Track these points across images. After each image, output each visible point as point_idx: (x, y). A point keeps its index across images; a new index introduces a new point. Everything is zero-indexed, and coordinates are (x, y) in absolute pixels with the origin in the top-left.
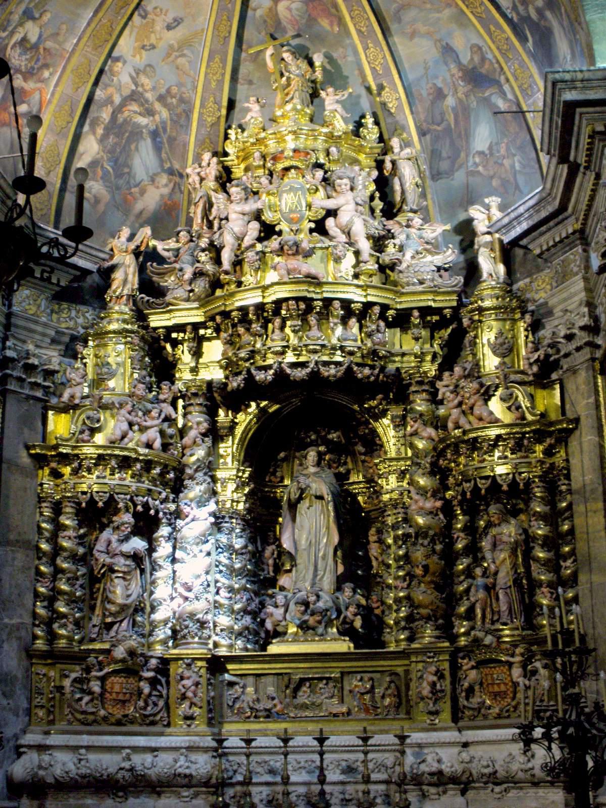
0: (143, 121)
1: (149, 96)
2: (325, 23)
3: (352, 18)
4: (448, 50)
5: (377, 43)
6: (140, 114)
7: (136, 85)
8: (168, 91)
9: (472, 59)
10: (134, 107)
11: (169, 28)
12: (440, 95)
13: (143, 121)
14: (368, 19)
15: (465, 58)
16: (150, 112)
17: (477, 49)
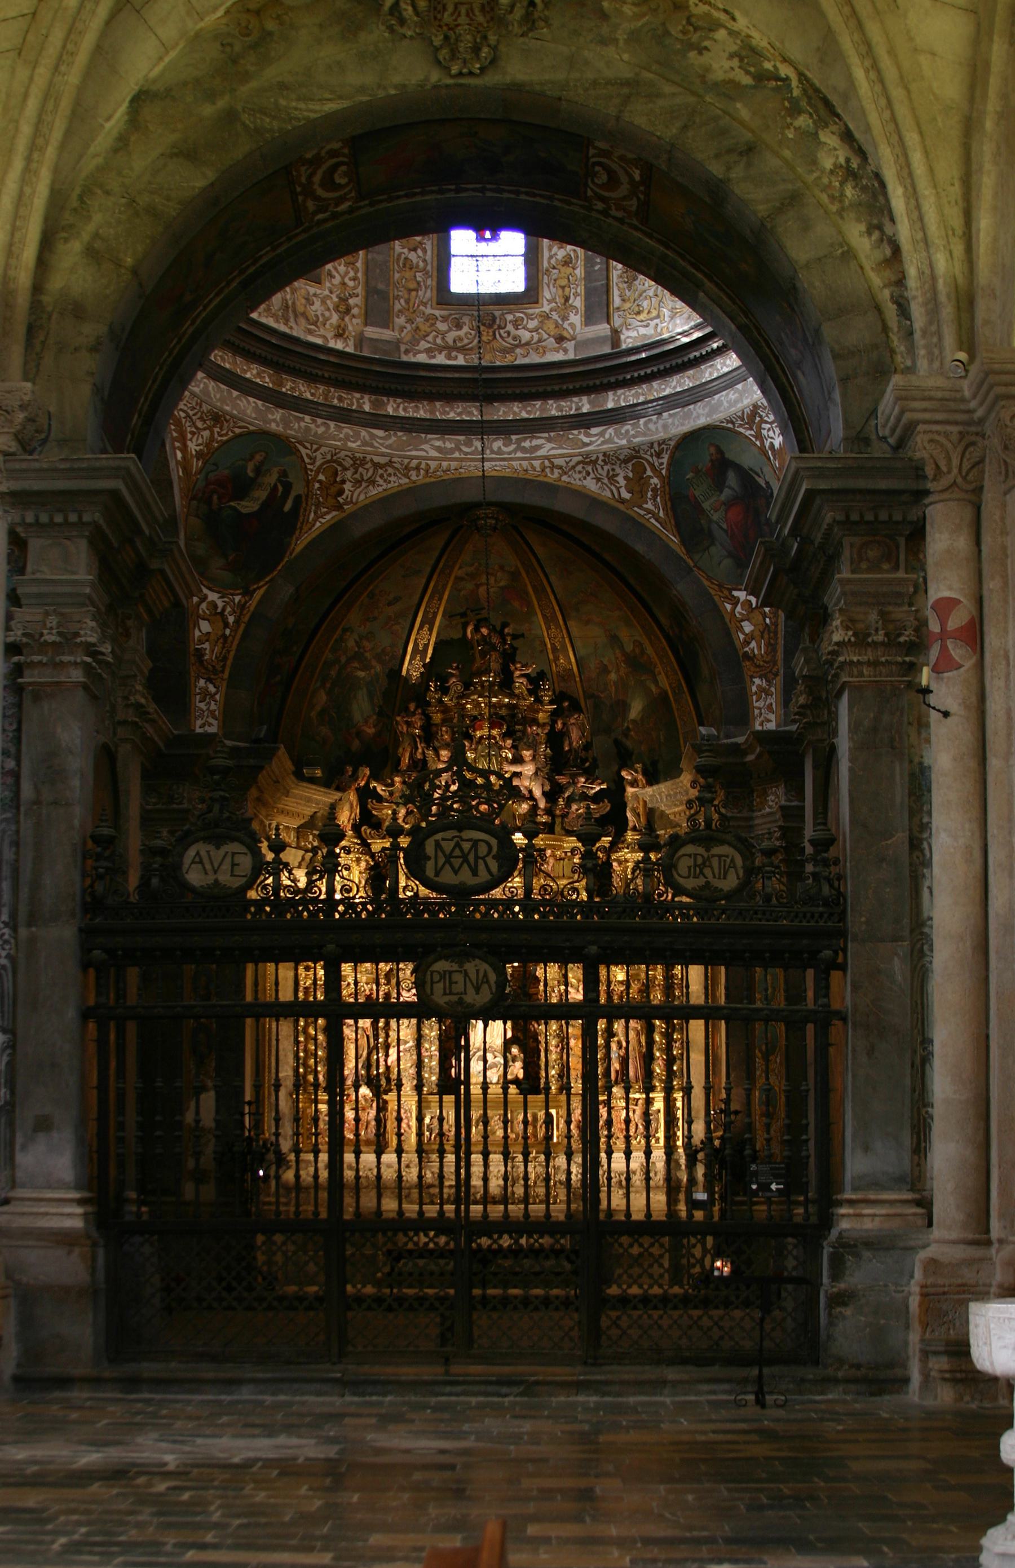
0: (361, 674)
1: (368, 655)
2: (516, 604)
3: (539, 606)
4: (614, 639)
5: (558, 626)
6: (361, 670)
7: (359, 647)
8: (383, 651)
9: (634, 650)
10: (356, 665)
11: (389, 604)
12: (605, 670)
13: (361, 674)
14: (553, 608)
15: (629, 648)
16: (365, 668)
17: (638, 644)
